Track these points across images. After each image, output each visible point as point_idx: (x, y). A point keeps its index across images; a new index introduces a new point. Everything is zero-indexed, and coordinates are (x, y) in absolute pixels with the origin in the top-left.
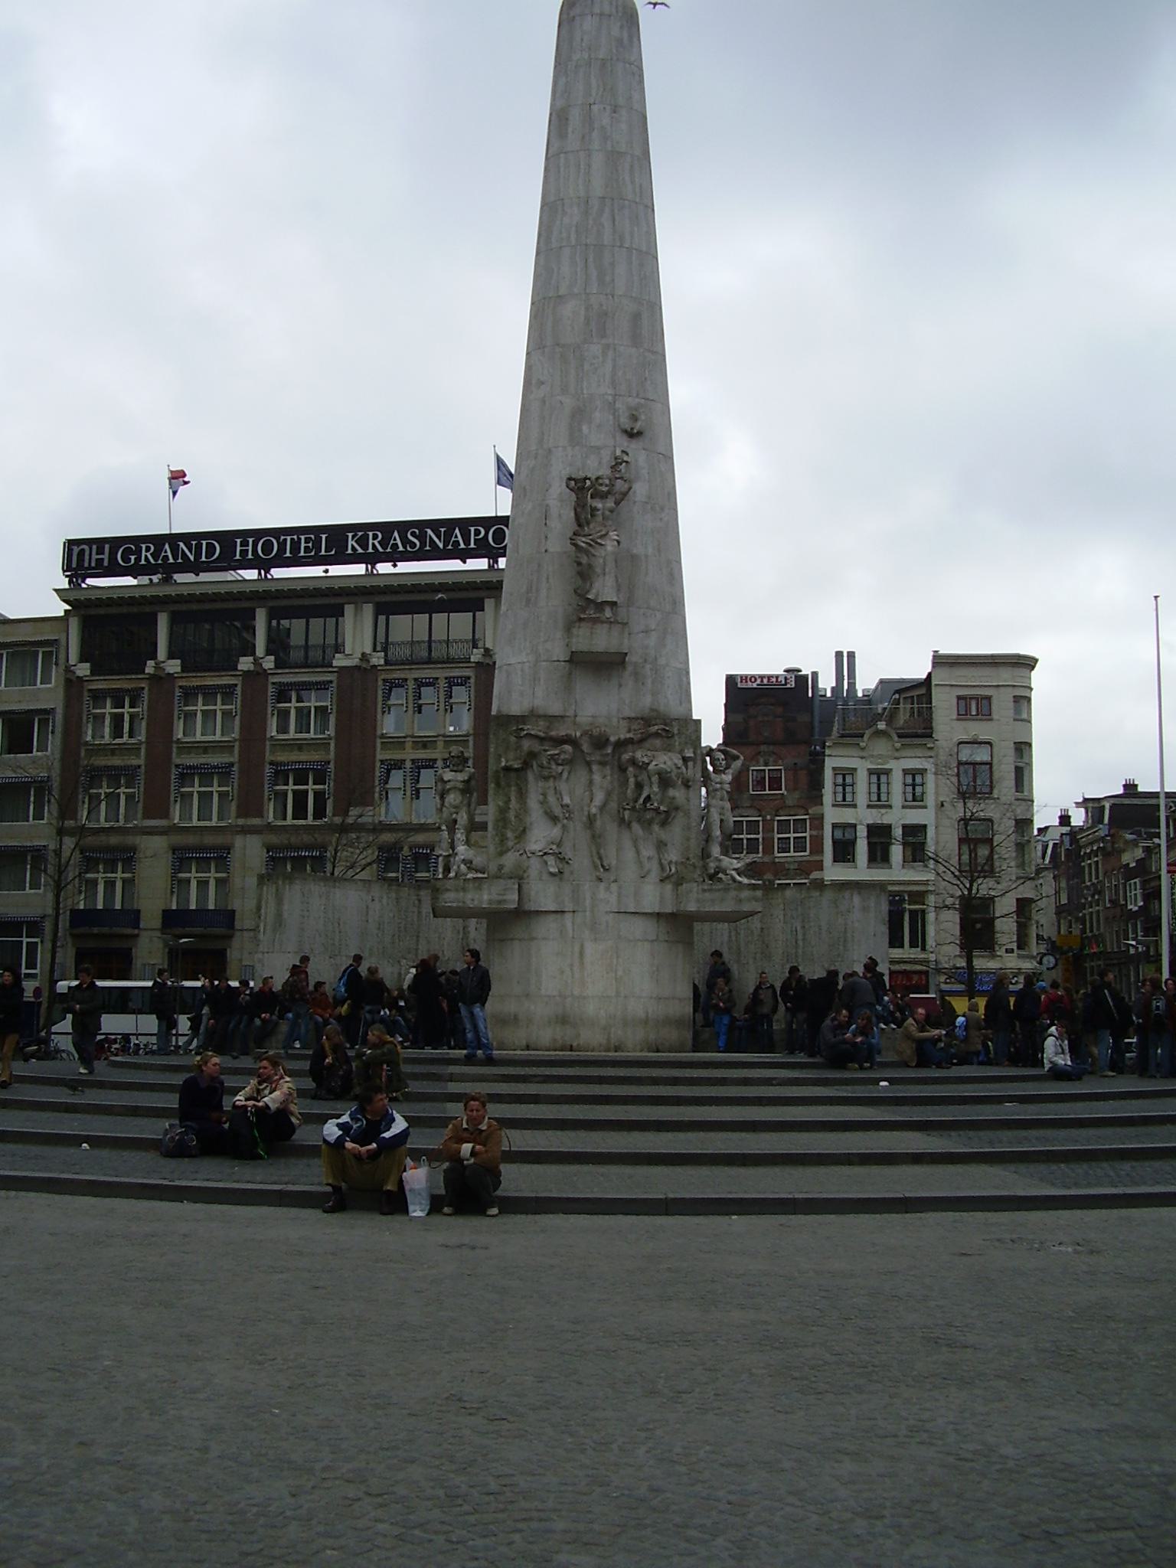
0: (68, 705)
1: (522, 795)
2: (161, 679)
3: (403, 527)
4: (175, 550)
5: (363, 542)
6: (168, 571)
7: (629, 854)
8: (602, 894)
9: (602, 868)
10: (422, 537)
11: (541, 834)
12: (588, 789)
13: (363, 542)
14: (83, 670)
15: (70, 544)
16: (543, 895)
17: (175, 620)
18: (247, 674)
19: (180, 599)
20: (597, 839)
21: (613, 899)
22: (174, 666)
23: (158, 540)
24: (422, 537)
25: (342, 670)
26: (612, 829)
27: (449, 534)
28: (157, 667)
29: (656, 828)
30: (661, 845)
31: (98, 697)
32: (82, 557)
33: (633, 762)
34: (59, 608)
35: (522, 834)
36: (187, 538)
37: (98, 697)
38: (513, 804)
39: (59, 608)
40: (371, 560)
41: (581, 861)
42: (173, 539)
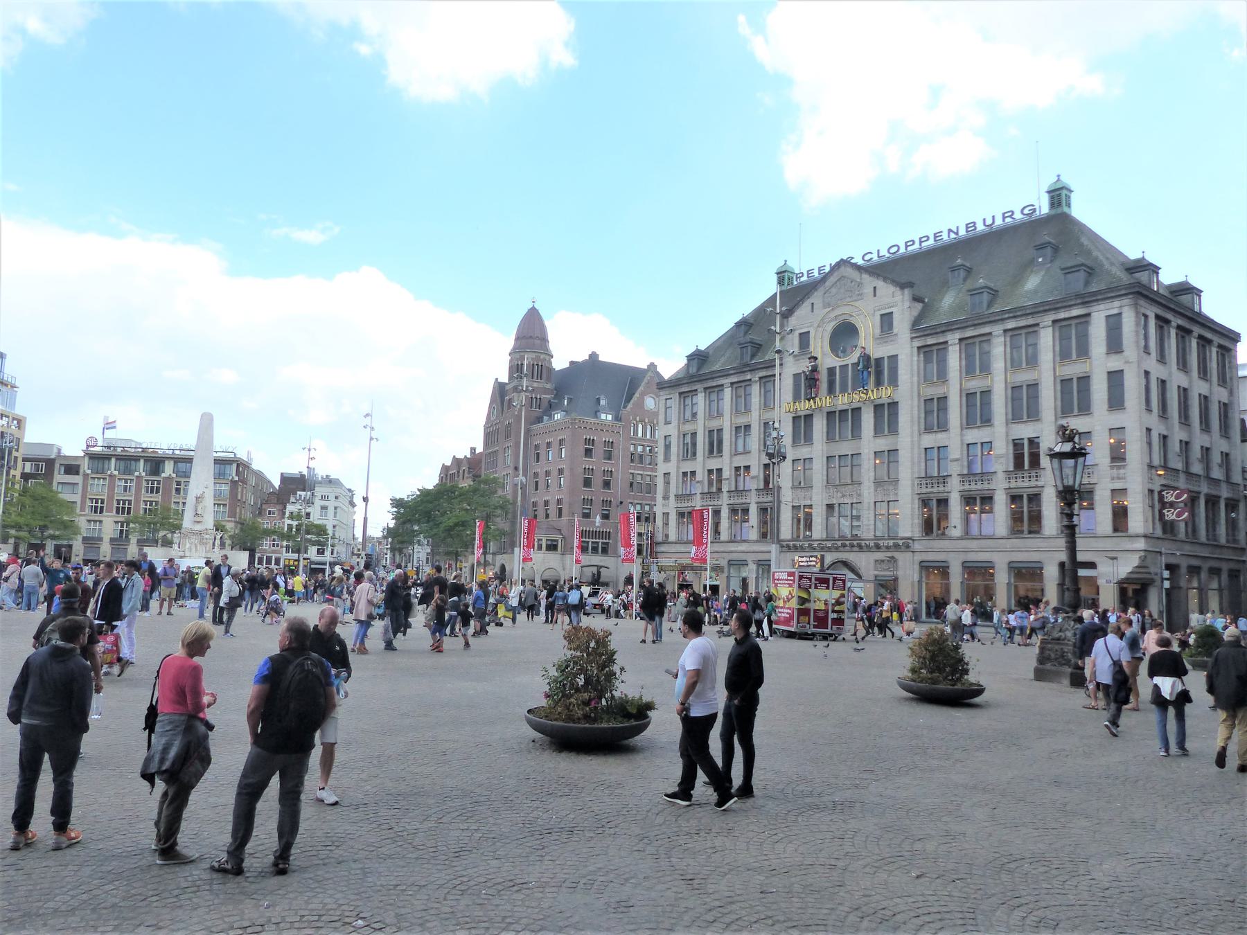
12: (195, 540)
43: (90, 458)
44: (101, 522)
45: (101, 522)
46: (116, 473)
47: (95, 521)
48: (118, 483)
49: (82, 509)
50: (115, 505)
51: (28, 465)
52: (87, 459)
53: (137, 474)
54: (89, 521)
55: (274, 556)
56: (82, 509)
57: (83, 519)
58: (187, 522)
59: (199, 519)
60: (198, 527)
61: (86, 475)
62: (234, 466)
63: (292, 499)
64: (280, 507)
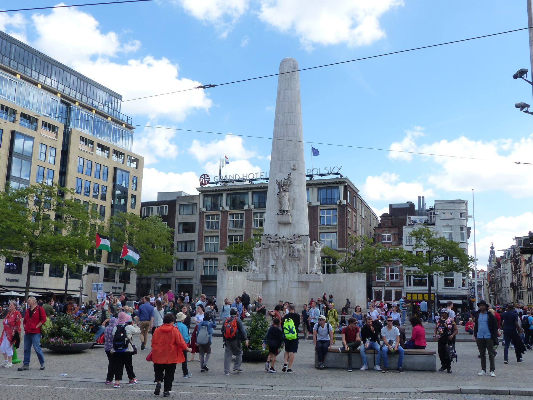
0: (200, 219)
1: (268, 254)
2: (224, 212)
7: (292, 268)
8: (285, 277)
9: (285, 269)
11: (272, 262)
12: (282, 253)
16: (272, 277)
17: (228, 194)
18: (246, 210)
19: (228, 190)
20: (284, 265)
21: (288, 278)
26: (288, 262)
28: (223, 208)
29: (297, 261)
30: (298, 266)
33: (292, 246)
34: (197, 193)
35: (268, 263)
38: (266, 256)
39: (197, 193)
41: (280, 270)
43: (205, 196)
44: (216, 259)
45: (216, 259)
46: (227, 208)
47: (211, 259)
48: (230, 218)
49: (200, 248)
50: (228, 241)
51: (155, 208)
52: (201, 197)
53: (246, 207)
54: (206, 259)
55: (393, 290)
56: (200, 248)
57: (201, 258)
58: (270, 227)
59: (284, 218)
60: (285, 233)
61: (201, 213)
62: (342, 189)
63: (408, 222)
64: (395, 231)
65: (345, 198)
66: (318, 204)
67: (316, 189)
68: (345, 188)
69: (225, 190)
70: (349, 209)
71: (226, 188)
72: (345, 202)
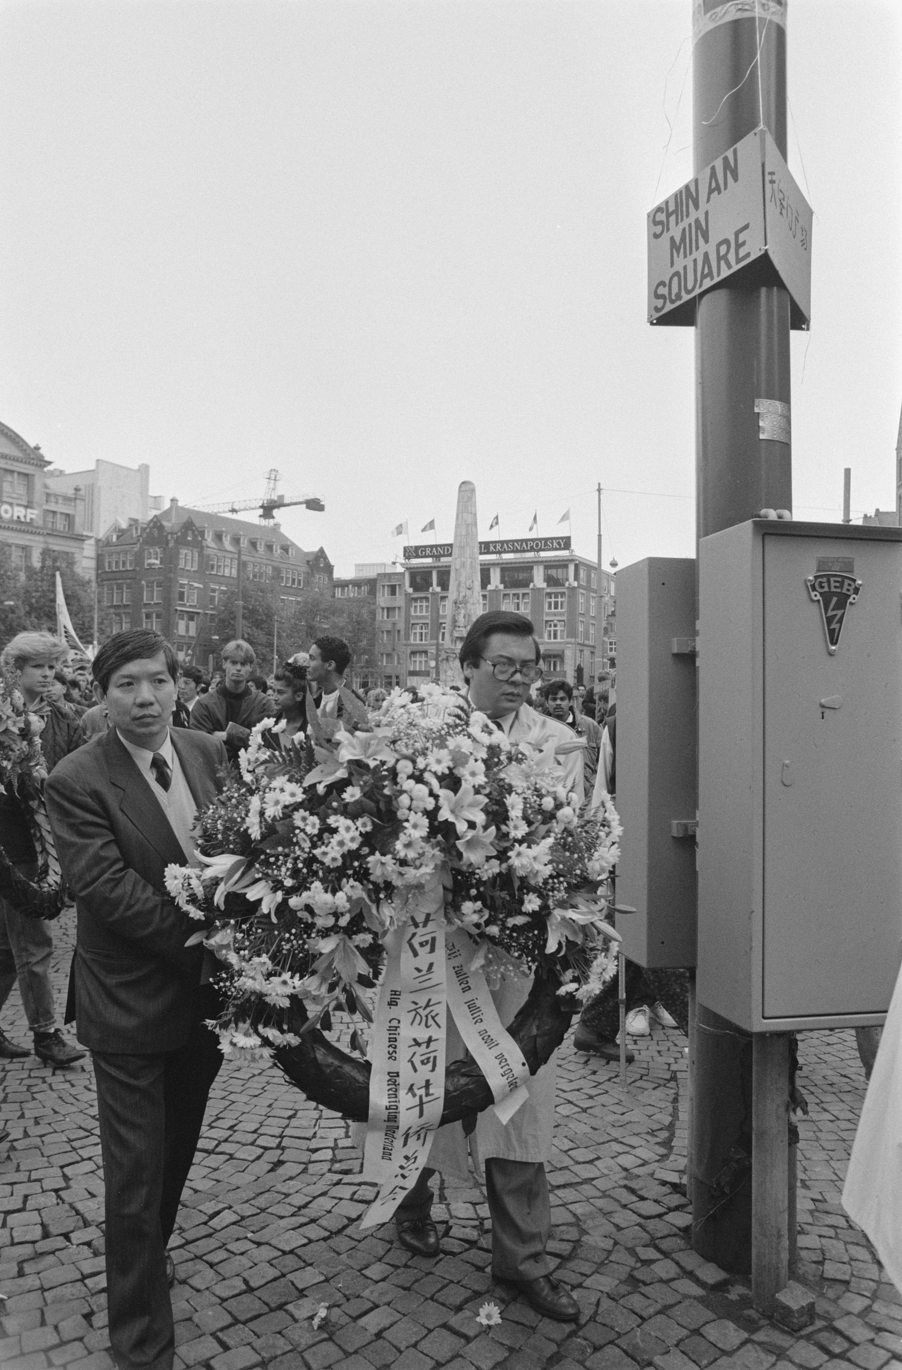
3: (507, 542)
4: (437, 550)
5: (495, 547)
6: (437, 557)
10: (513, 545)
13: (495, 547)
14: (410, 590)
15: (405, 548)
17: (438, 572)
19: (439, 567)
22: (438, 589)
23: (432, 547)
24: (513, 545)
25: (490, 591)
27: (522, 545)
31: (416, 600)
32: (411, 552)
36: (440, 546)
37: (416, 600)
40: (500, 553)
42: (436, 546)
62: (572, 568)
65: (576, 578)
66: (544, 585)
67: (541, 568)
68: (576, 566)
69: (435, 567)
70: (581, 591)
71: (437, 564)
72: (575, 584)
